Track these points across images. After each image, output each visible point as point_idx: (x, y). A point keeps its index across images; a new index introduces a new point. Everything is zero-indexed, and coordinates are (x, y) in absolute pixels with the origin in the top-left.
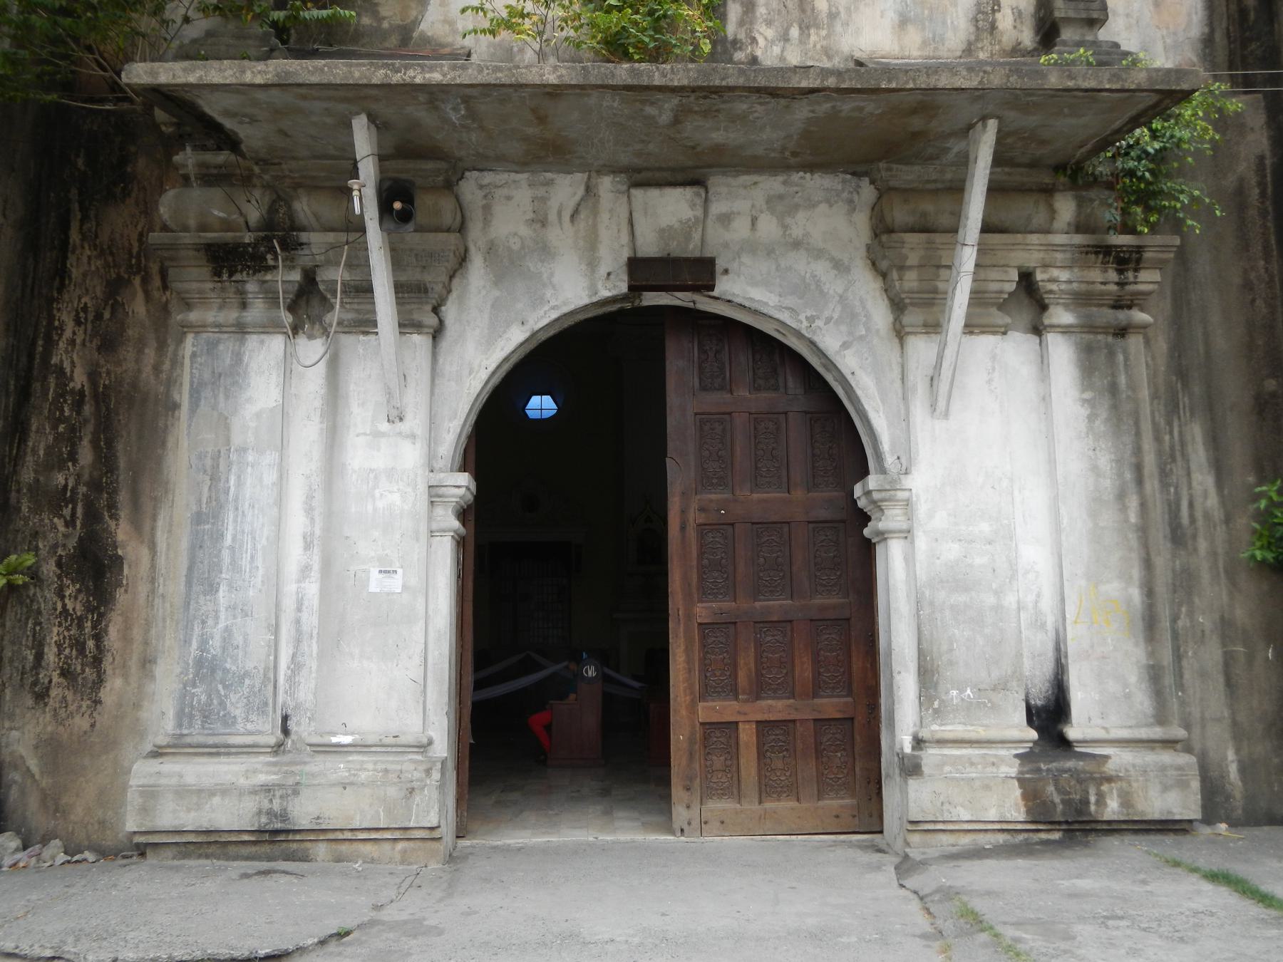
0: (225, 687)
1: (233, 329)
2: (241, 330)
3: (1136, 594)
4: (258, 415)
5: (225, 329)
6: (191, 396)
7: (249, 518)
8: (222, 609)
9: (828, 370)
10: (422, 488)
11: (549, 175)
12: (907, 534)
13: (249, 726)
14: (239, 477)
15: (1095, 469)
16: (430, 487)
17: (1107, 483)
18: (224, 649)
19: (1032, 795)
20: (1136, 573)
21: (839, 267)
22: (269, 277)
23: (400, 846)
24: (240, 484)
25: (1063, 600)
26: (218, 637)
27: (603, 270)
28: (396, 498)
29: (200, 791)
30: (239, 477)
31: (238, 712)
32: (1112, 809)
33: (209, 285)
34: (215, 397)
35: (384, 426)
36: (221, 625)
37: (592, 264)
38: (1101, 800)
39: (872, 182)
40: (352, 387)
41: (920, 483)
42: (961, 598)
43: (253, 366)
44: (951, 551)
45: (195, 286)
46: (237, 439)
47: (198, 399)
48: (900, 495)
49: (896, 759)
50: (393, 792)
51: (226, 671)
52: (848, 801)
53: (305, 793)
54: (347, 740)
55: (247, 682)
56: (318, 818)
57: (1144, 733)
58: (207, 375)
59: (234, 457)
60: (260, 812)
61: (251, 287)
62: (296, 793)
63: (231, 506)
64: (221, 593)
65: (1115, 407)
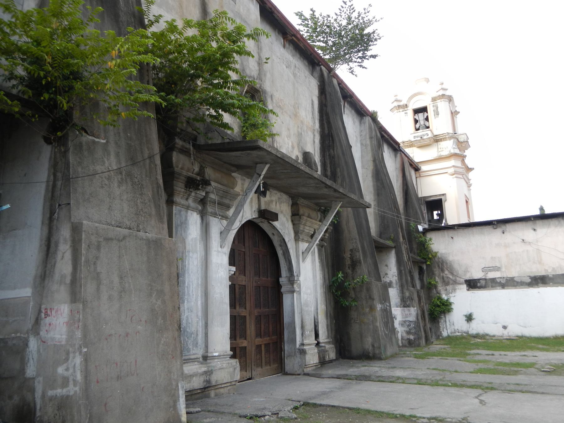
0: (188, 338)
1: (185, 207)
2: (188, 208)
3: (325, 307)
4: (192, 239)
5: (184, 207)
6: (175, 229)
7: (191, 277)
8: (186, 309)
9: (281, 246)
10: (228, 270)
11: (245, 178)
12: (299, 293)
13: (194, 352)
14: (188, 261)
15: (320, 278)
16: (229, 270)
17: (322, 281)
18: (187, 324)
19: (319, 356)
20: (325, 303)
21: (287, 220)
22: (198, 192)
23: (229, 388)
24: (189, 264)
25: (317, 309)
26: (185, 319)
27: (254, 209)
28: (222, 273)
29: (191, 376)
30: (188, 261)
31: (191, 347)
32: (327, 359)
33: (183, 190)
34: (182, 231)
35: (220, 249)
36: (186, 315)
37: (252, 207)
38: (326, 357)
39: (292, 199)
40: (213, 235)
41: (301, 278)
42: (306, 309)
43: (190, 222)
44: (306, 296)
45: (180, 189)
46: (188, 248)
47: (177, 230)
48: (299, 282)
49: (297, 350)
50: (231, 370)
51: (187, 332)
52: (277, 365)
53: (214, 373)
54: (216, 354)
55: (193, 336)
56: (217, 381)
57: (326, 341)
58: (179, 222)
59: (187, 254)
60: (204, 381)
61: (193, 194)
62: (212, 373)
63: (187, 272)
64: (185, 304)
65: (322, 264)
